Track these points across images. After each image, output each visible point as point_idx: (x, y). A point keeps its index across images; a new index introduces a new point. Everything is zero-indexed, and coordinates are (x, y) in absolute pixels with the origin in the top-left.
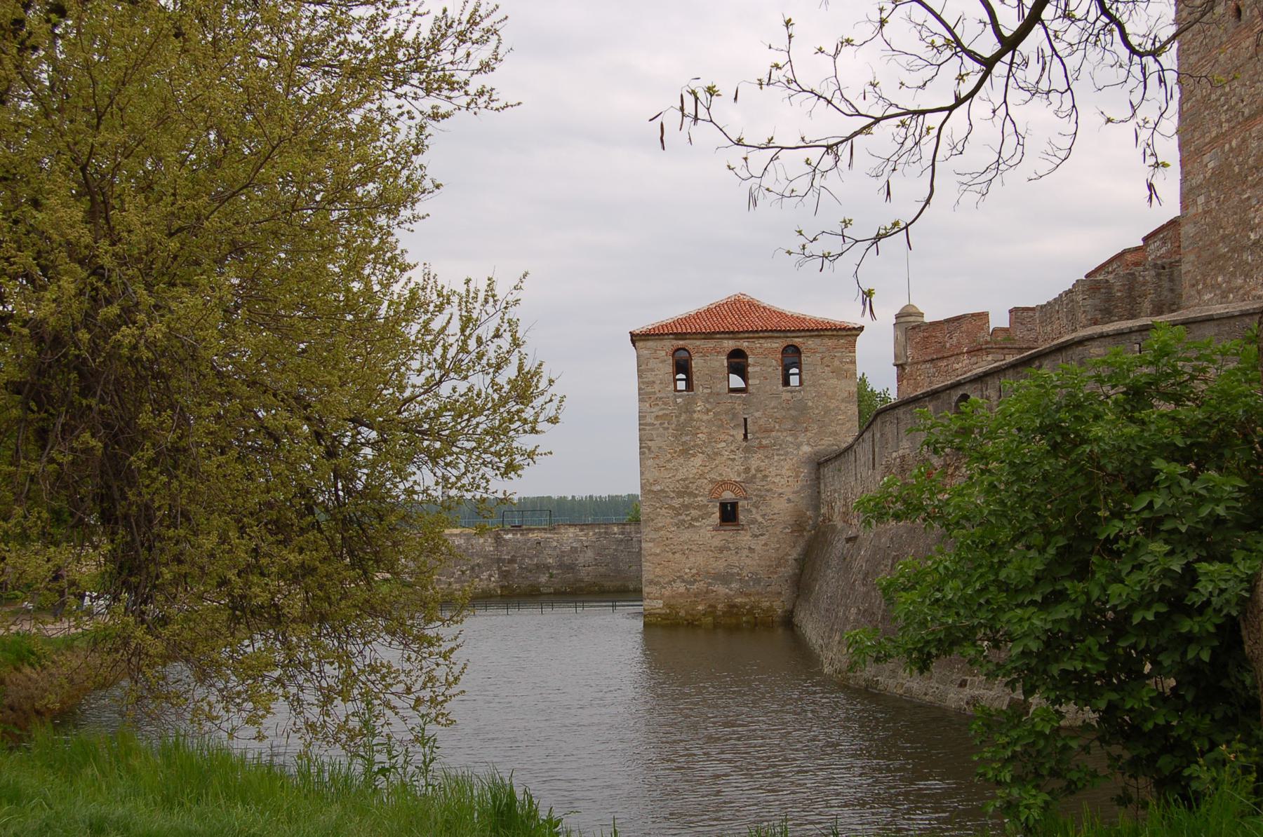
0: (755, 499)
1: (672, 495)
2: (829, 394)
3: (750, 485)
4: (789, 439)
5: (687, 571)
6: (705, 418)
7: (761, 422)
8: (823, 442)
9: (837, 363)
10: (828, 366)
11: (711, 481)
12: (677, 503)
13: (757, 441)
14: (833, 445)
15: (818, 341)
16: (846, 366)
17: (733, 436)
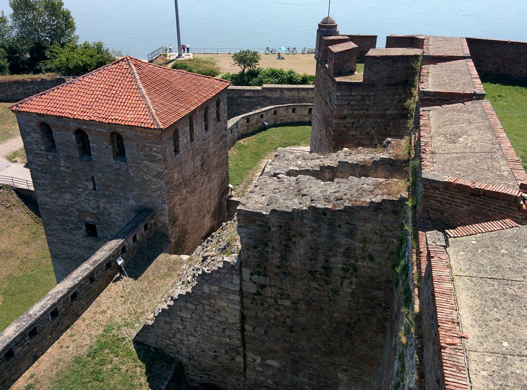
0: (105, 225)
1: (57, 213)
2: (145, 170)
3: (102, 217)
4: (122, 194)
5: (73, 255)
6: (67, 171)
7: (103, 180)
8: (143, 200)
9: (147, 149)
10: (142, 151)
11: (78, 210)
12: (60, 218)
13: (102, 192)
14: (149, 203)
15: (133, 132)
16: (154, 154)
17: (86, 185)
